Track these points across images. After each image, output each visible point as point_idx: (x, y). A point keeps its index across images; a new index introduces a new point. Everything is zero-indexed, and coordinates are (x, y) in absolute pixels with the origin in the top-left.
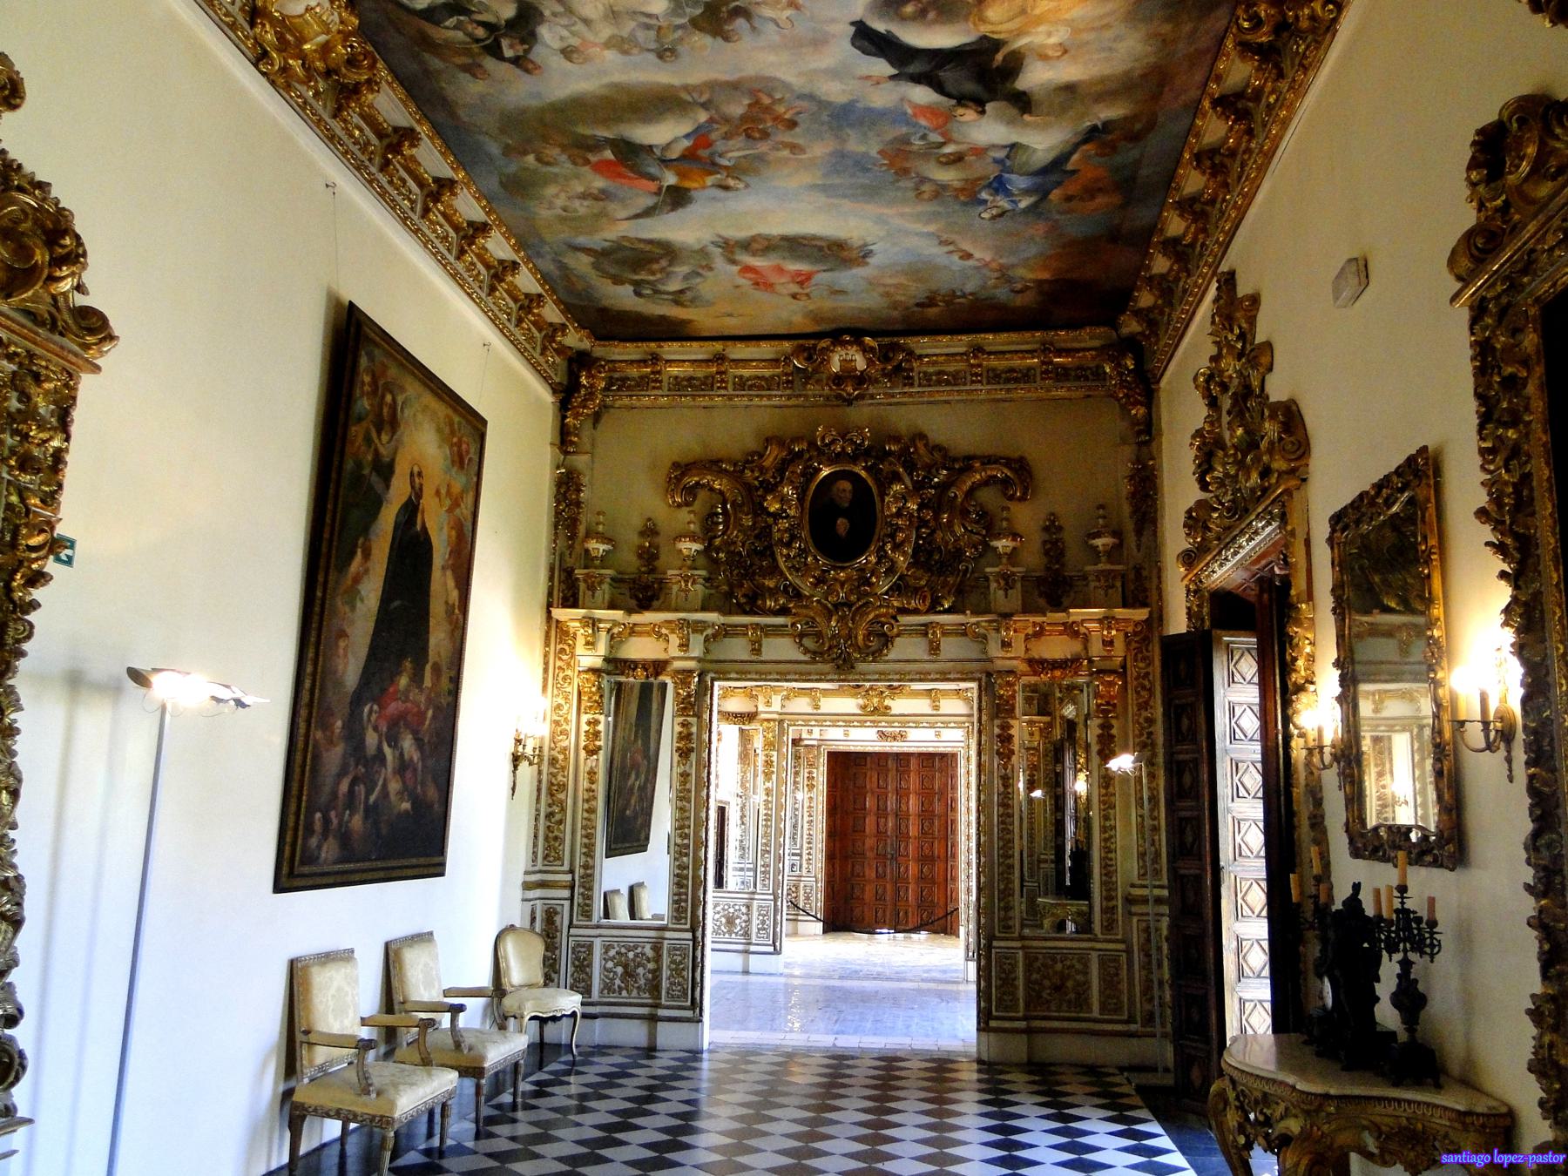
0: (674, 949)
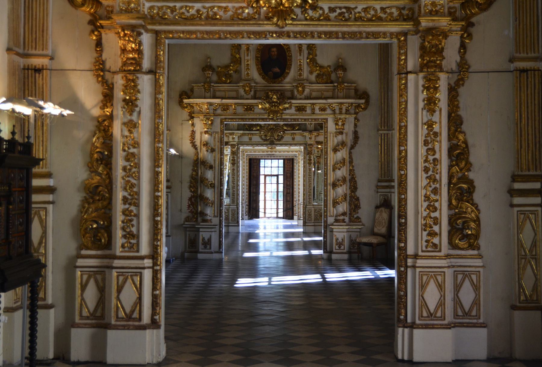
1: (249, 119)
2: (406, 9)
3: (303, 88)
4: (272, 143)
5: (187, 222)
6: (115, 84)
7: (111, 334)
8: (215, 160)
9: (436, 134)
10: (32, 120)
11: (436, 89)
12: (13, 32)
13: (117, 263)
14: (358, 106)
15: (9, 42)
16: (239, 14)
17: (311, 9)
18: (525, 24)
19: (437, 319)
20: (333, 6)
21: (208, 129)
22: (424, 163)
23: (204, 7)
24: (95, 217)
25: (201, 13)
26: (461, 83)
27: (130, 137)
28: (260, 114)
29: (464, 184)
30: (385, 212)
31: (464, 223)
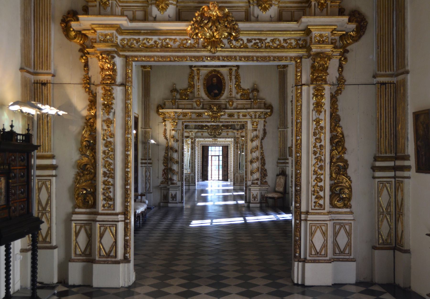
0: (192, 176)
1: (199, 121)
2: (301, 40)
3: (232, 102)
4: (215, 137)
5: (162, 184)
6: (97, 93)
7: (96, 267)
8: (178, 147)
9: (322, 128)
10: (36, 118)
11: (322, 96)
12: (25, 57)
13: (99, 218)
14: (266, 113)
15: (21, 63)
16: (184, 44)
17: (235, 40)
18: (384, 50)
19: (321, 256)
20: (250, 38)
21: (174, 127)
22: (313, 148)
23: (159, 39)
24: (84, 186)
25: (157, 43)
26: (339, 92)
27: (108, 130)
28: (206, 118)
29: (341, 162)
30: (283, 179)
31: (341, 190)
